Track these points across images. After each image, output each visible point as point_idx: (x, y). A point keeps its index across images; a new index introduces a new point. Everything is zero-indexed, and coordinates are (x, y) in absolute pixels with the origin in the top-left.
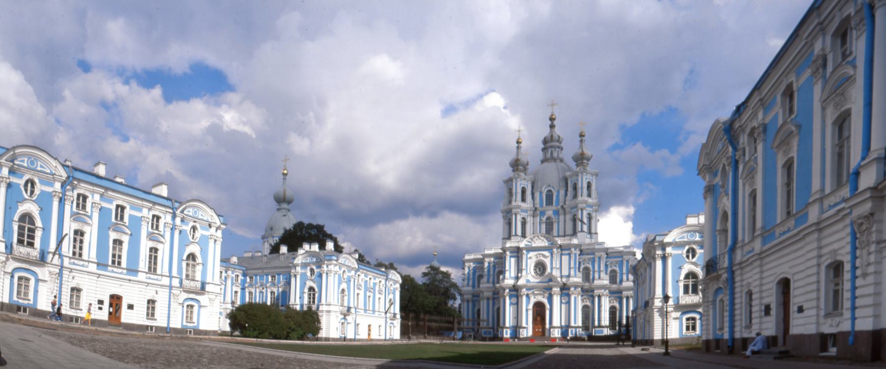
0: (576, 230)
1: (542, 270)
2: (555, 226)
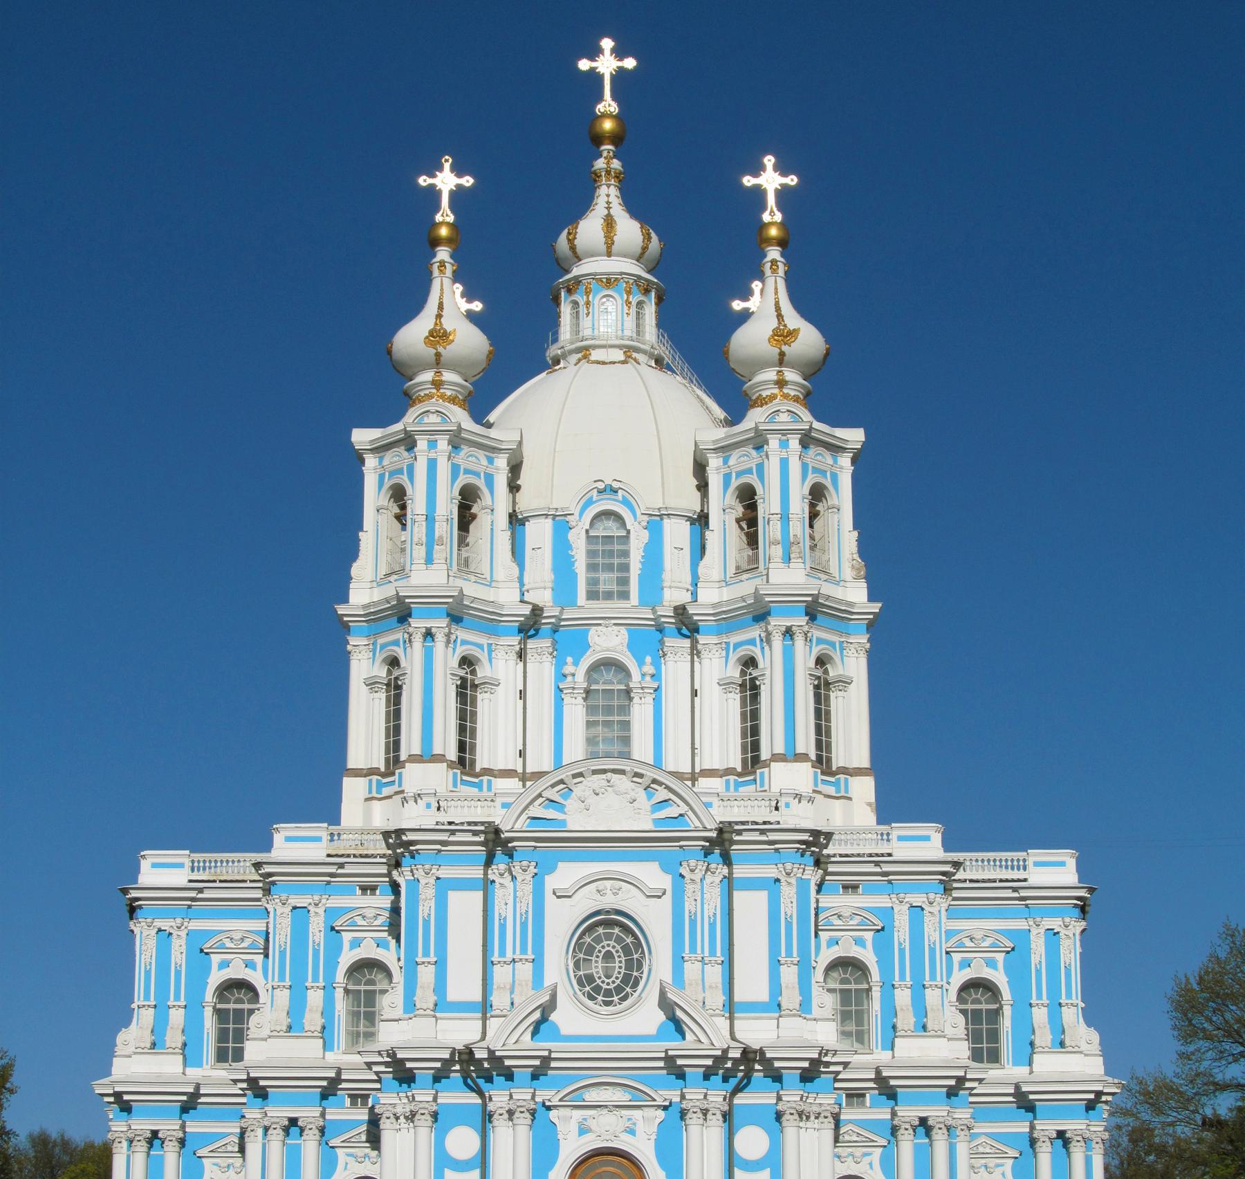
0: (756, 746)
1: (619, 965)
2: (641, 713)
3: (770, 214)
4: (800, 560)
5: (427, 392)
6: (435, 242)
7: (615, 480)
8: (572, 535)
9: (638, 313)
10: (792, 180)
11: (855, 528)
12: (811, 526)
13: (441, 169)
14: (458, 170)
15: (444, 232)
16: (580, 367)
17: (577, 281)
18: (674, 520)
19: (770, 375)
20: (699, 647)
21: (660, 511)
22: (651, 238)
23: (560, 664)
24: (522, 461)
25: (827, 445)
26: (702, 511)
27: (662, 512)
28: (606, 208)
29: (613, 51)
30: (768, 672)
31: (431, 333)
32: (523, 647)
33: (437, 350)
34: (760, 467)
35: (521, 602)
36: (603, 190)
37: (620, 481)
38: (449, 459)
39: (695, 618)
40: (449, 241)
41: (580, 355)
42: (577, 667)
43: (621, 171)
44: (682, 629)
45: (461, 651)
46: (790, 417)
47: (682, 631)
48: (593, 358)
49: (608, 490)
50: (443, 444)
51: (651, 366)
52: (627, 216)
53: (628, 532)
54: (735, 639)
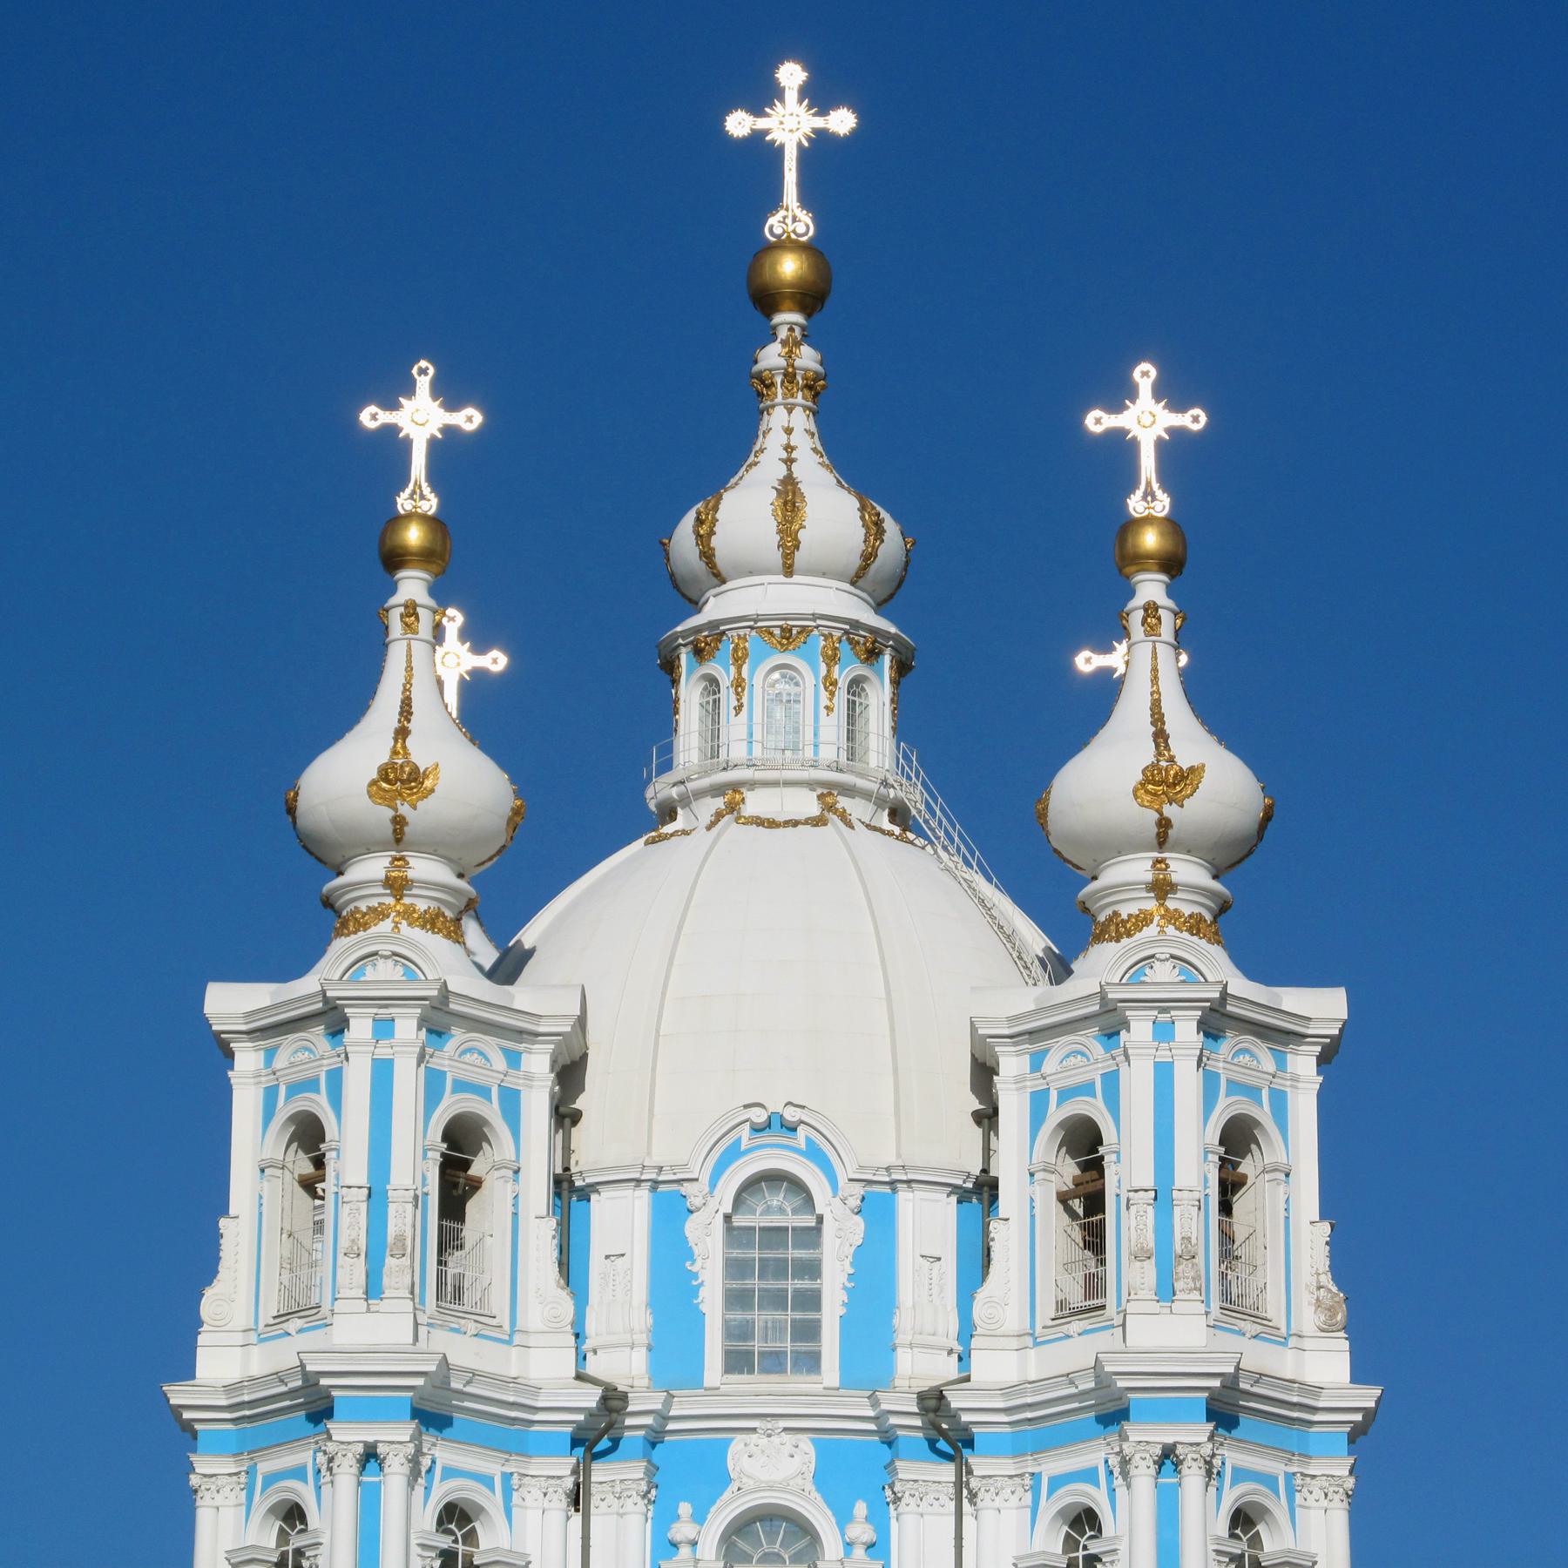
3: (1144, 498)
4: (1195, 1295)
5: (374, 903)
6: (394, 560)
7: (789, 1103)
8: (692, 1228)
9: (851, 705)
10: (1196, 419)
11: (1323, 1217)
12: (1226, 1208)
13: (409, 389)
14: (449, 393)
15: (414, 536)
16: (719, 836)
17: (717, 631)
18: (921, 1193)
19: (1138, 868)
20: (974, 1483)
21: (890, 1175)
22: (884, 531)
23: (663, 1519)
24: (585, 1057)
25: (1261, 1030)
26: (985, 1171)
27: (895, 1177)
29: (805, 92)
30: (1123, 1547)
31: (385, 773)
32: (581, 1480)
33: (396, 810)
34: (1111, 1081)
35: (580, 1377)
36: (777, 419)
37: (803, 1107)
38: (421, 1059)
39: (965, 1418)
40: (426, 557)
41: (719, 803)
42: (702, 1525)
43: (816, 373)
44: (938, 1441)
45: (443, 1491)
46: (1177, 970)
47: (937, 1445)
48: (749, 810)
49: (776, 1123)
50: (407, 1027)
51: (875, 829)
52: (829, 478)
53: (820, 1219)
54: (1053, 1465)
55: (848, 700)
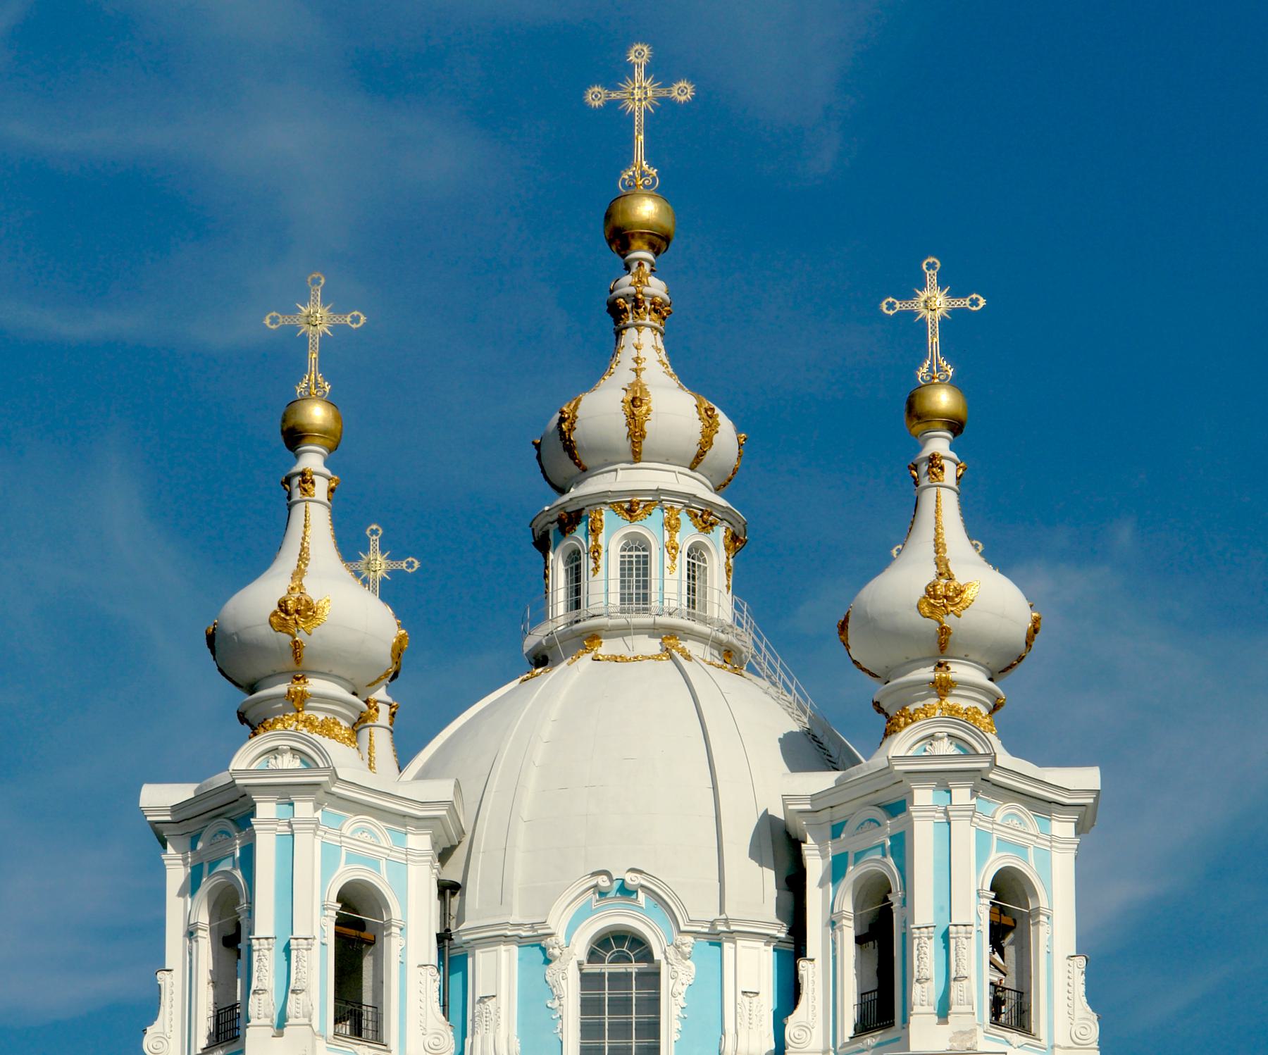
28: (635, 370)
36: (630, 336)
52: (673, 382)
55: (688, 562)
